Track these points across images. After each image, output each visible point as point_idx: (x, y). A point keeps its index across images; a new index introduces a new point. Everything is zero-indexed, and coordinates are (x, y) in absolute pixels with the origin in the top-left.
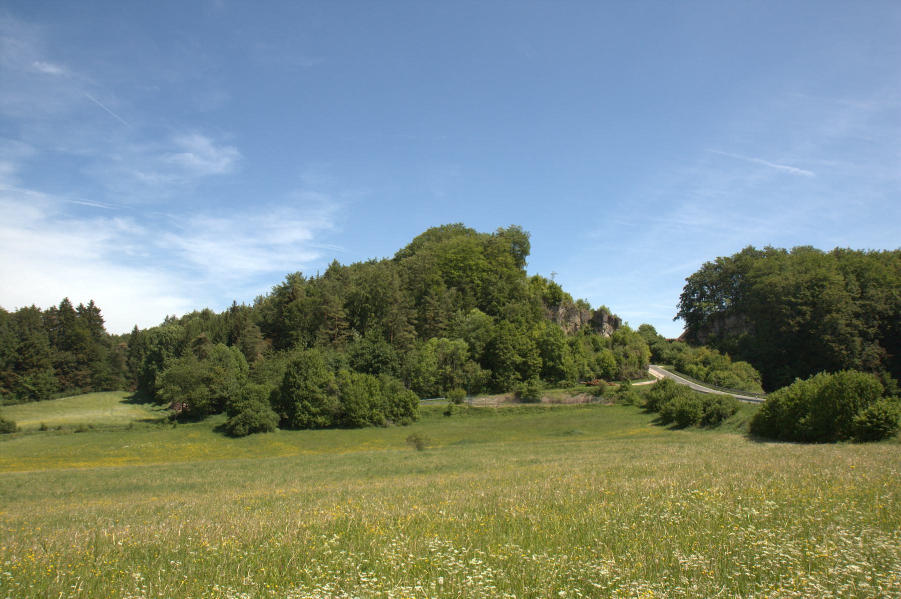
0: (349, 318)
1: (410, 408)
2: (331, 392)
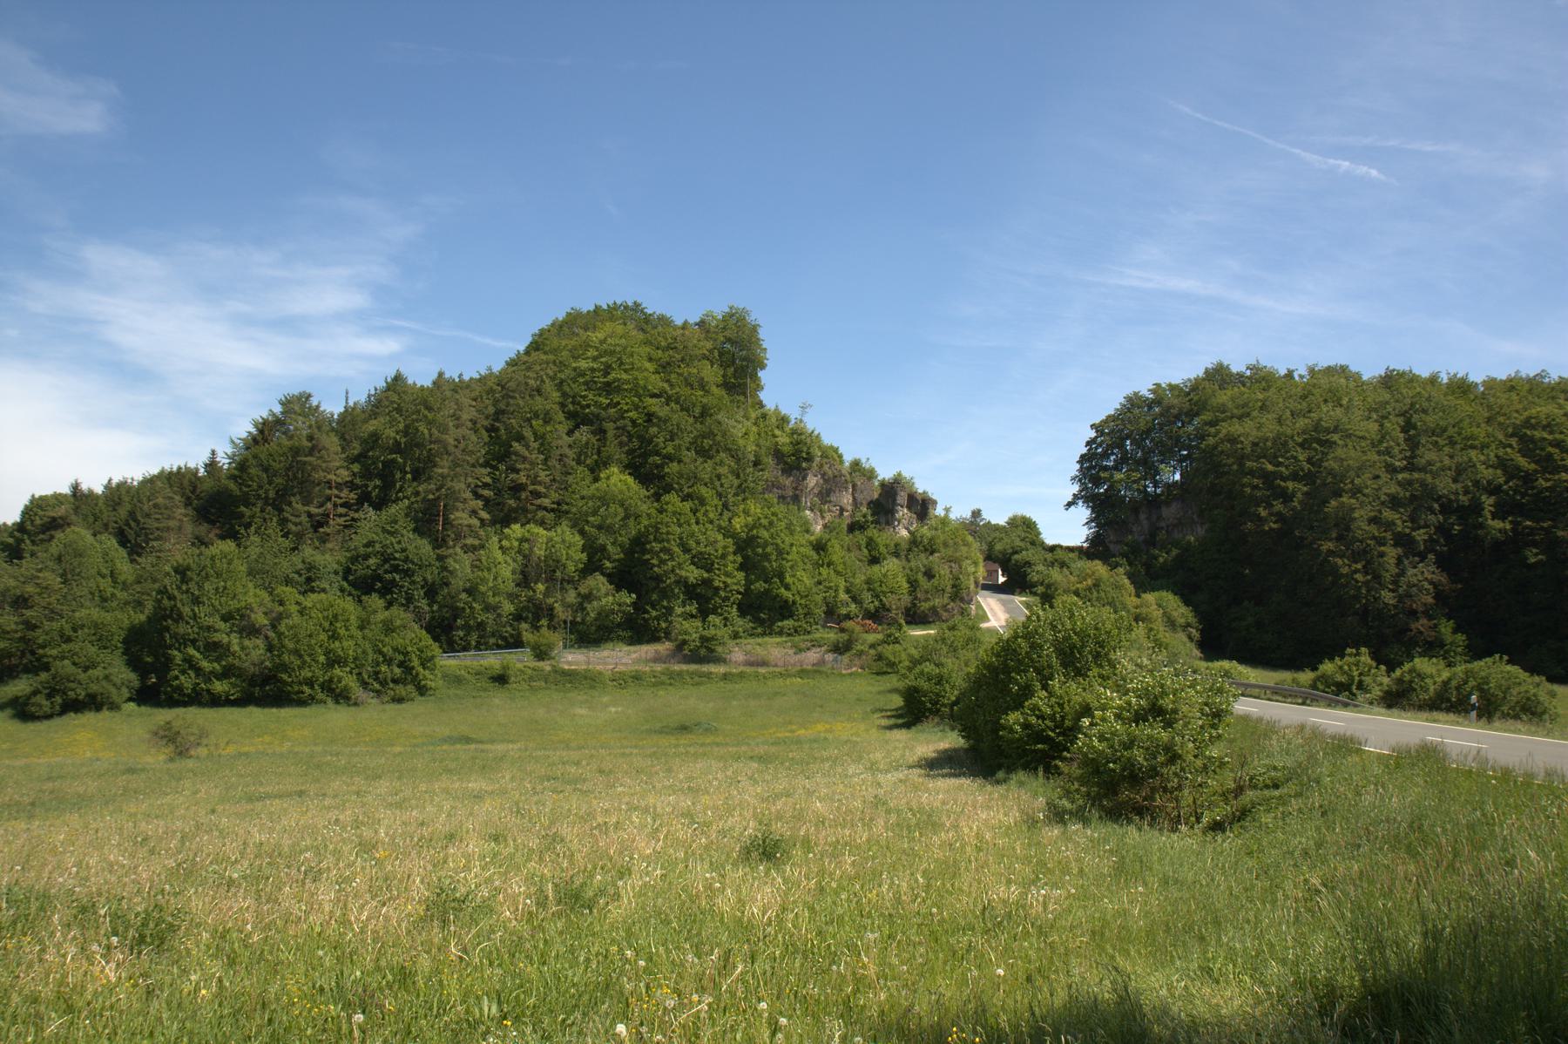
0: (358, 481)
1: (413, 668)
2: (252, 631)
